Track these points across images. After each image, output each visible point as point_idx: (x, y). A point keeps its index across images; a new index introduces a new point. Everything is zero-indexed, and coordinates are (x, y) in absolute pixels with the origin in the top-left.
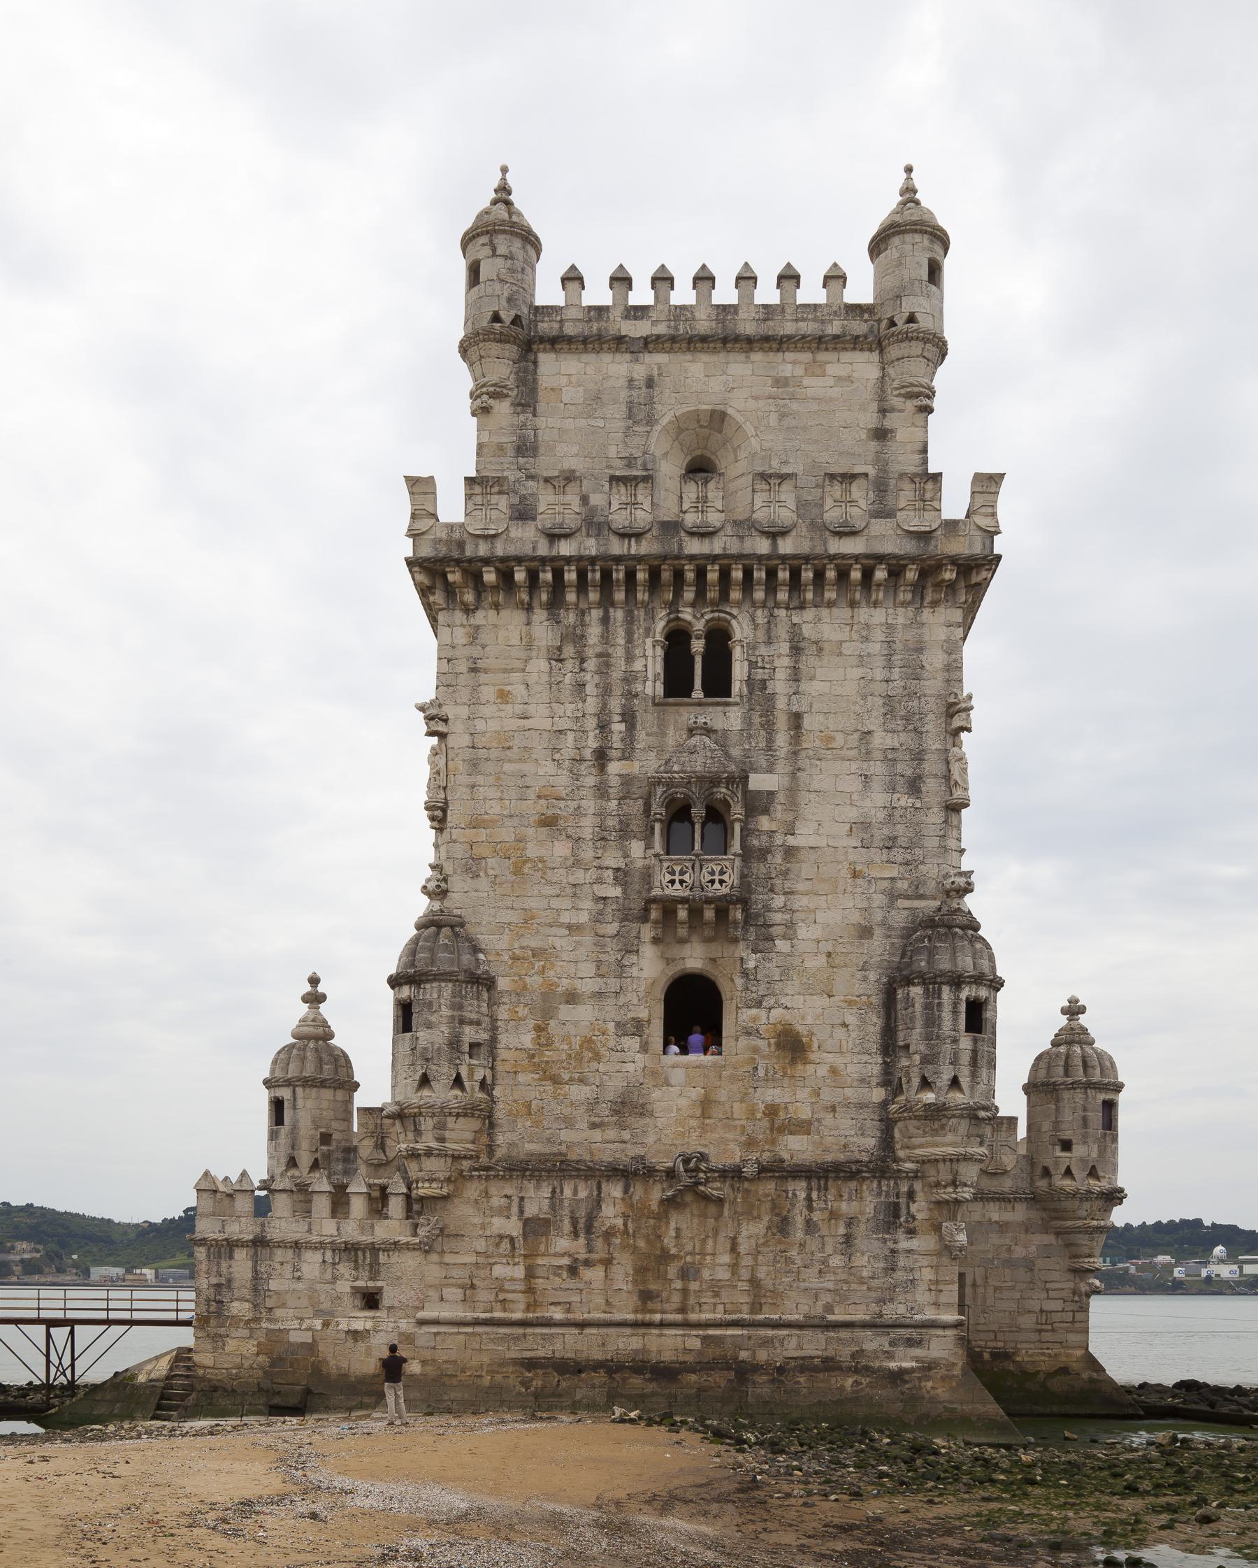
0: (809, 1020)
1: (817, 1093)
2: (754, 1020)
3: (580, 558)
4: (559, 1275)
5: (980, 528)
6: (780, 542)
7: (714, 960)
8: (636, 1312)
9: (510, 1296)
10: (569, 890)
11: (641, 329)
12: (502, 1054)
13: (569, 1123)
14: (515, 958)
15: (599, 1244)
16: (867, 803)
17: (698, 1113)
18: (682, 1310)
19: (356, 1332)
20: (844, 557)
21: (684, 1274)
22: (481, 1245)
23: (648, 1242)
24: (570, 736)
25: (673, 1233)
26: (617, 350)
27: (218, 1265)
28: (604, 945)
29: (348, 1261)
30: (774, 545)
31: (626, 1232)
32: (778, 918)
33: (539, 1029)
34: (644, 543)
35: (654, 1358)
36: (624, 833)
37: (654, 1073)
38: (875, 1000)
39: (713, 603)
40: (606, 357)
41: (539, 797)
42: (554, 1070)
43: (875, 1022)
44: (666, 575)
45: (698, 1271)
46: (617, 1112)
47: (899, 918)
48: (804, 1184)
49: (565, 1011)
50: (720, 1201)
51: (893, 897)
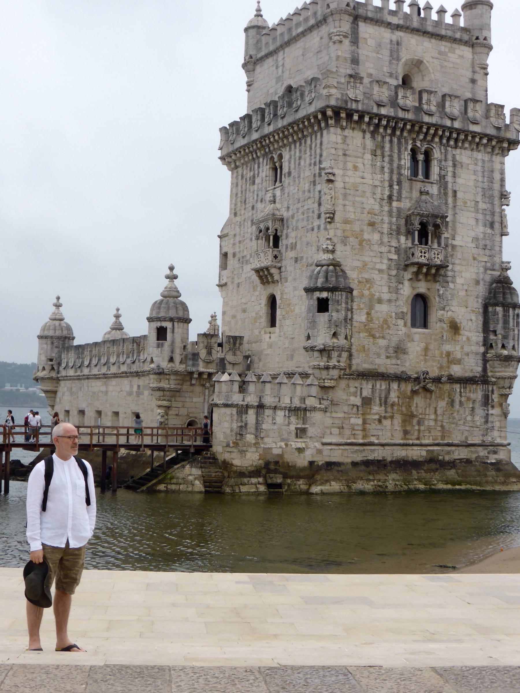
0: (460, 317)
1: (462, 348)
2: (443, 315)
3: (390, 117)
4: (374, 423)
5: (515, 129)
6: (454, 122)
7: (429, 289)
8: (402, 439)
9: (357, 432)
10: (379, 254)
11: (395, 20)
12: (355, 324)
13: (379, 355)
14: (359, 282)
15: (389, 409)
16: (477, 230)
17: (424, 354)
18: (418, 439)
19: (299, 448)
20: (475, 133)
21: (419, 423)
22: (346, 409)
23: (406, 408)
24: (379, 188)
25: (415, 405)
26: (387, 27)
27: (241, 417)
28: (391, 280)
29: (295, 415)
30: (452, 123)
31: (399, 404)
32: (450, 274)
33: (368, 314)
34: (410, 114)
35: (410, 459)
36: (398, 233)
37: (409, 336)
38: (481, 310)
39: (429, 141)
40: (382, 29)
41: (368, 213)
42: (373, 333)
43: (481, 319)
44: (417, 128)
45: (423, 422)
46: (396, 352)
47: (488, 278)
48: (458, 385)
49: (378, 307)
50: (430, 392)
51: (486, 269)
